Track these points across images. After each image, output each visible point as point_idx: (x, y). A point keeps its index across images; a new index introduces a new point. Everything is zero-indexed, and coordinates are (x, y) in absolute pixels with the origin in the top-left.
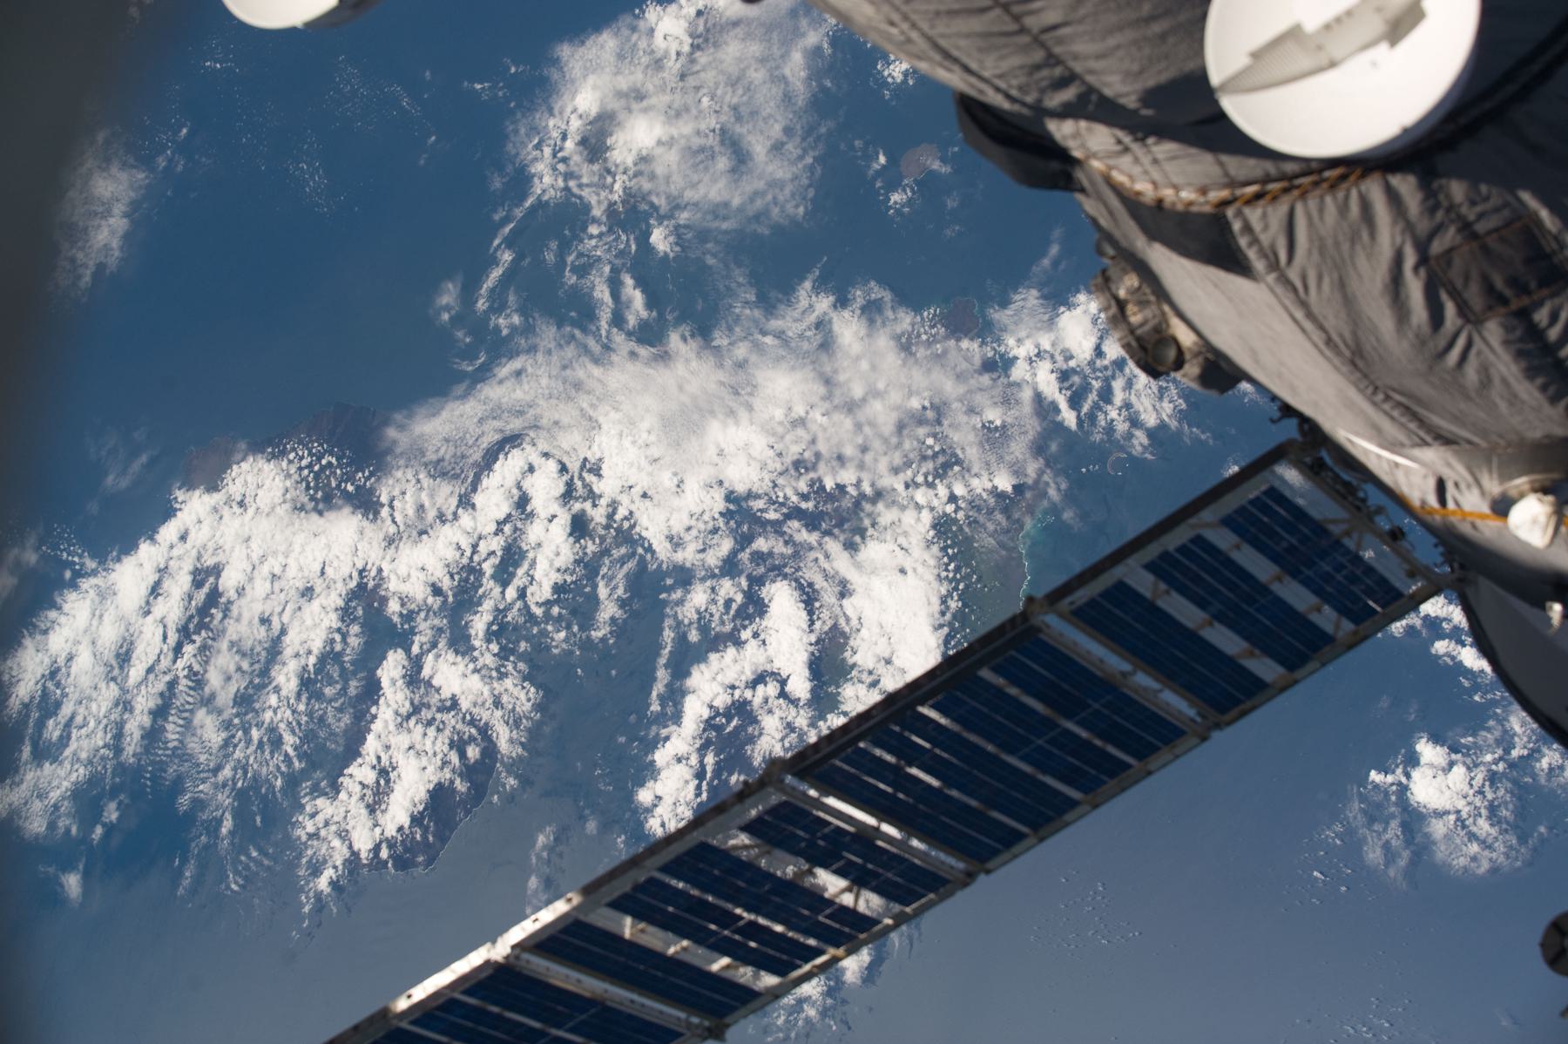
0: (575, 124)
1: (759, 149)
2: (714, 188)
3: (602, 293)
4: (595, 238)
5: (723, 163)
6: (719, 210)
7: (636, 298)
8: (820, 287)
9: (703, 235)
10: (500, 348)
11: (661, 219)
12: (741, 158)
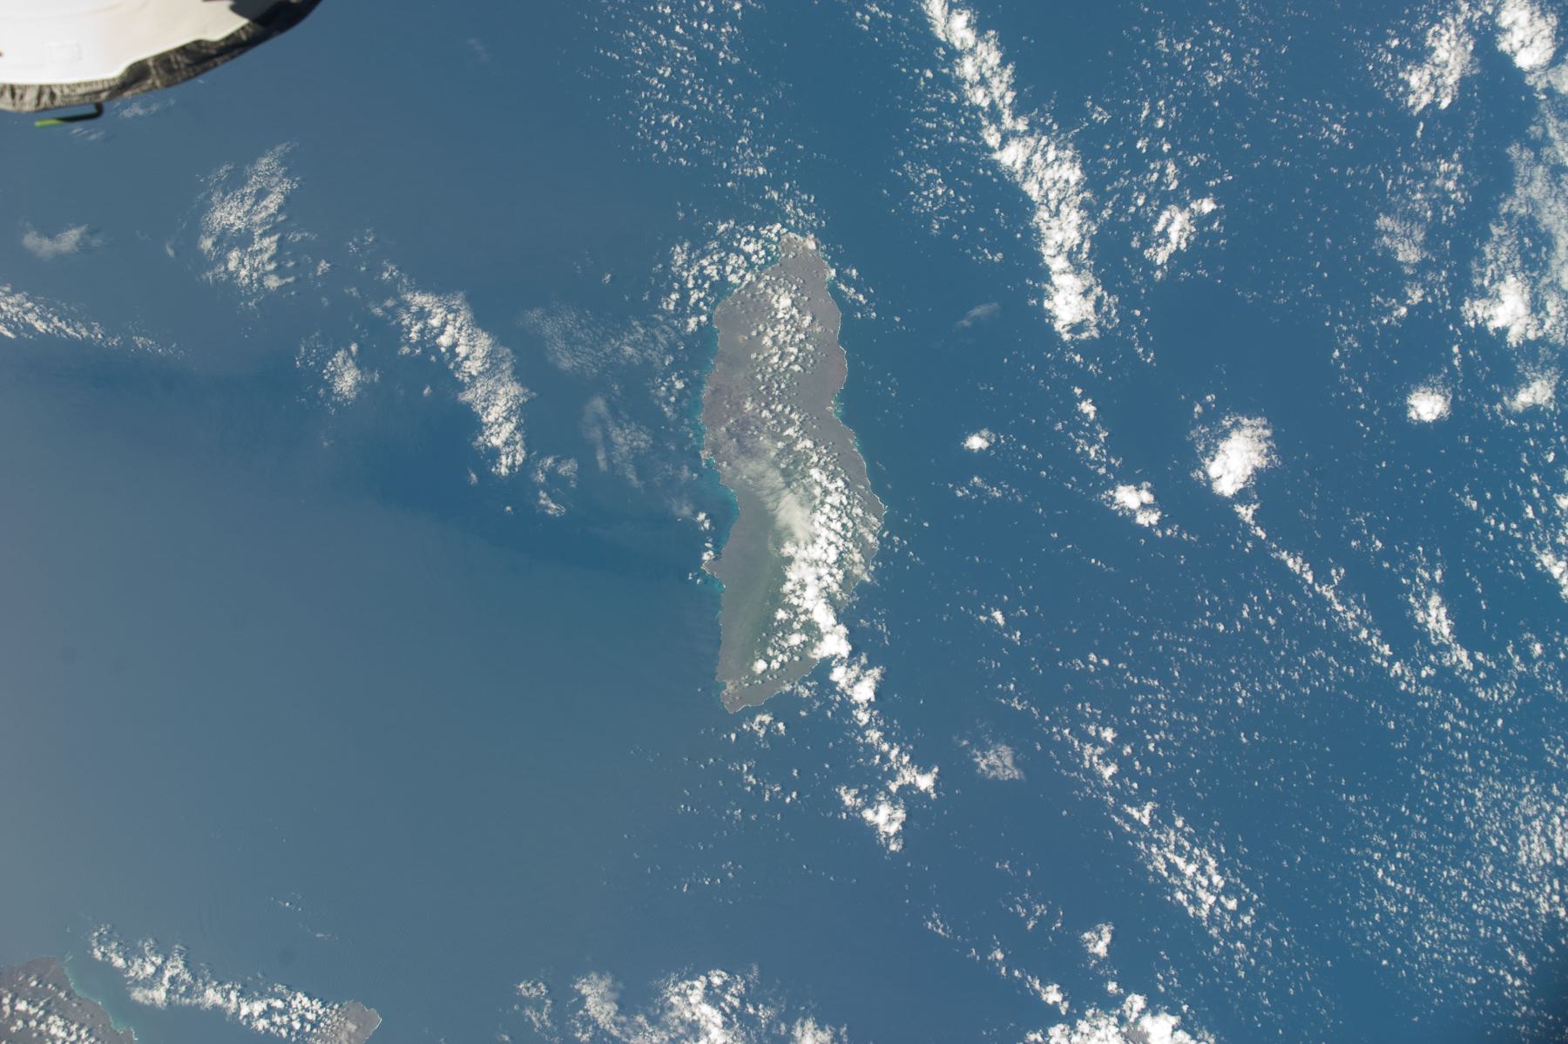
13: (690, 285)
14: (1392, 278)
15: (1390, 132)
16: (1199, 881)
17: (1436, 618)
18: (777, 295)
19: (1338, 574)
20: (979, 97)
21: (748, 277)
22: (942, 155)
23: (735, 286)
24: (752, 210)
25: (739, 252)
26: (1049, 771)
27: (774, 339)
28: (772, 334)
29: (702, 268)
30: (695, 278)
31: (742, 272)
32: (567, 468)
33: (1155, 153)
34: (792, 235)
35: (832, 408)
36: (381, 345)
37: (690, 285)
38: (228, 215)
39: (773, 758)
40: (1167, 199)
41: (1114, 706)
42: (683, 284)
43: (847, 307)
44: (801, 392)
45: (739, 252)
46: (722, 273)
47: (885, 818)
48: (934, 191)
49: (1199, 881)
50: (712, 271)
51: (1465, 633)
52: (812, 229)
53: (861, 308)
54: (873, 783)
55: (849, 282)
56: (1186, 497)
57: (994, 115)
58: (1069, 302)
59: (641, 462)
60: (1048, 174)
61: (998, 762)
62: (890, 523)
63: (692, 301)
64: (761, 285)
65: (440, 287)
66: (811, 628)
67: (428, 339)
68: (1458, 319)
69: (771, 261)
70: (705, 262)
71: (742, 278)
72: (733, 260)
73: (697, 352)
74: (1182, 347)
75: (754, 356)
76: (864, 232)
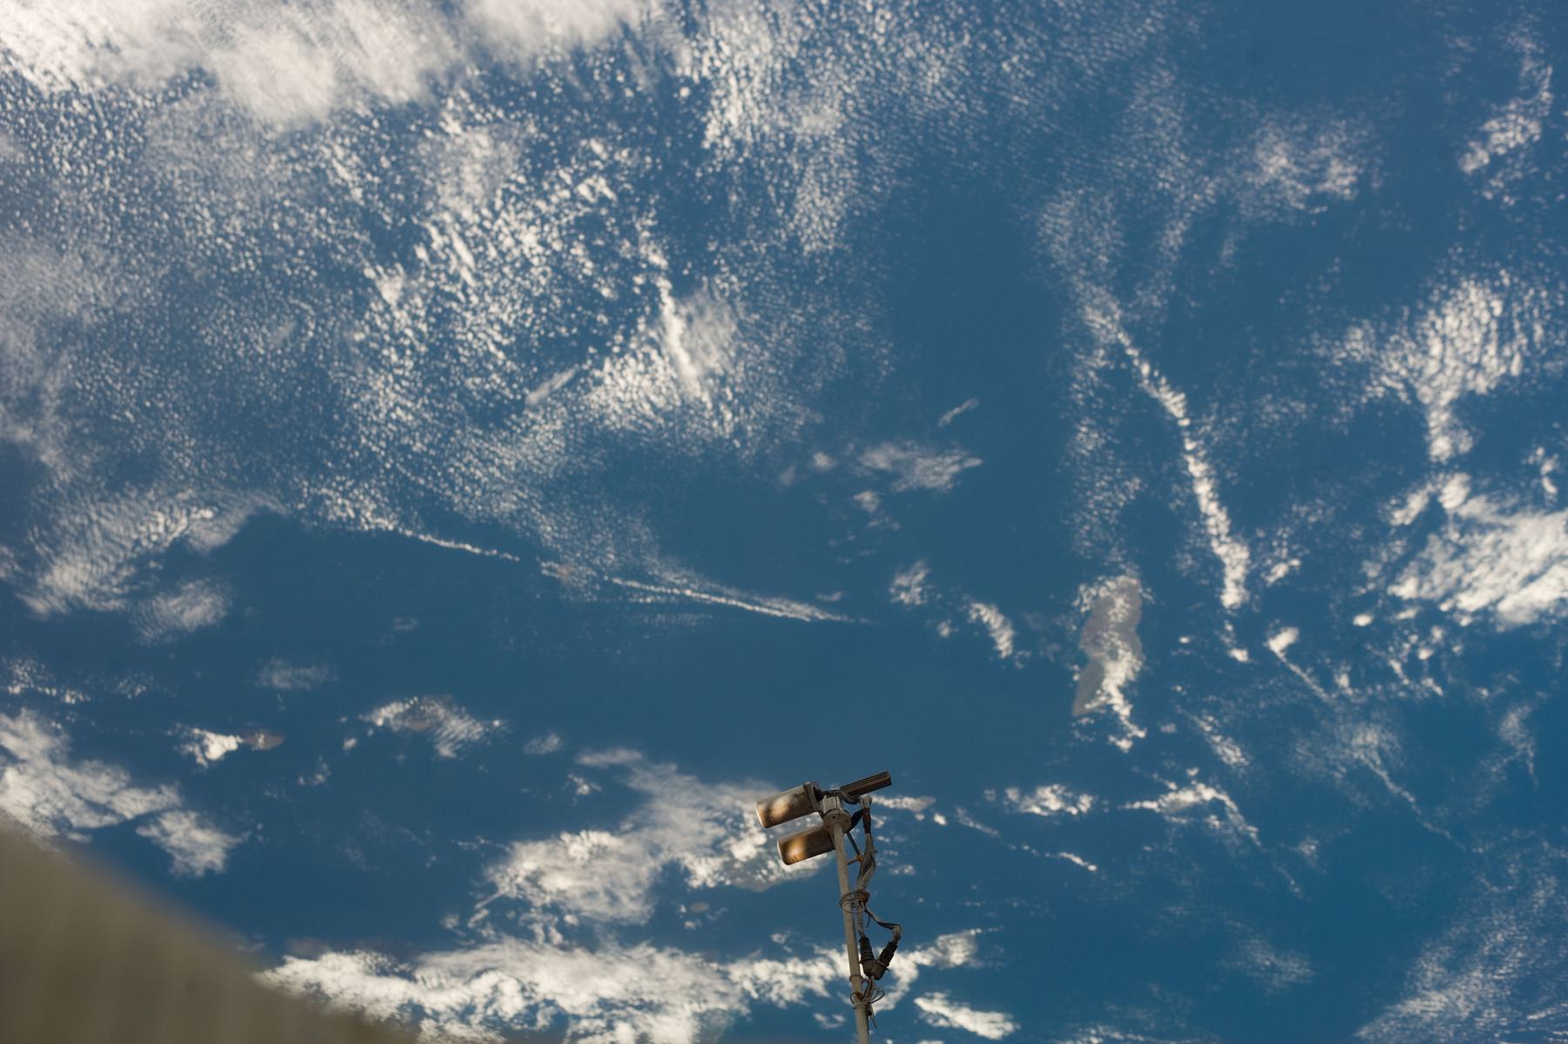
0: (523, 873)
1: (625, 900)
2: (601, 907)
3: (538, 929)
4: (534, 914)
5: (604, 899)
6: (600, 914)
7: (557, 937)
8: (652, 944)
9: (594, 921)
10: (481, 941)
11: (570, 912)
12: (614, 899)
14: (1364, 580)
15: (1381, 532)
16: (1232, 755)
17: (1344, 681)
18: (1117, 597)
19: (1309, 670)
20: (1214, 531)
22: (1193, 551)
24: (1113, 571)
26: (1186, 729)
32: (1028, 654)
33: (1280, 546)
35: (1132, 630)
36: (960, 619)
38: (902, 581)
39: (1087, 730)
40: (1278, 560)
41: (1215, 709)
44: (1121, 628)
47: (1124, 744)
48: (1187, 562)
49: (1232, 755)
51: (1352, 685)
54: (1122, 734)
56: (1261, 654)
57: (1218, 536)
58: (1231, 596)
59: (1055, 654)
60: (1234, 558)
61: (1170, 728)
62: (1146, 663)
65: (987, 602)
66: (1109, 696)
67: (979, 619)
68: (1384, 592)
73: (1082, 620)
74: (1269, 605)
76: (1155, 572)
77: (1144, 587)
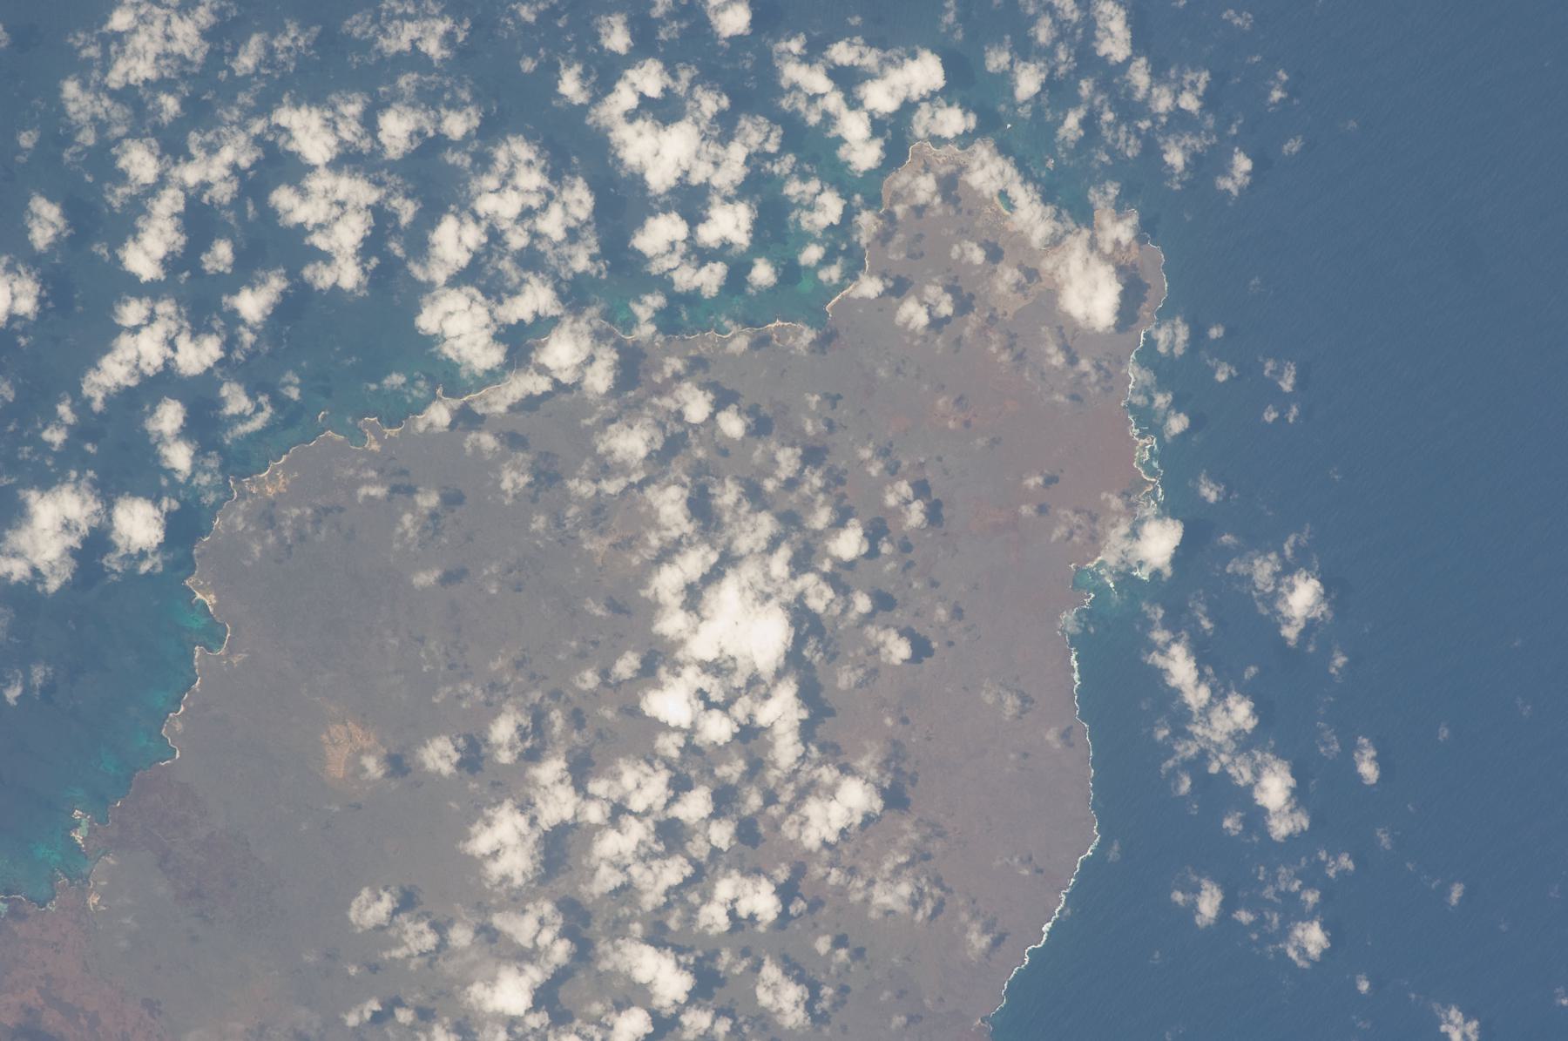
13: (144, 257)
21: (562, 353)
23: (448, 377)
25: (576, 148)
27: (560, 849)
28: (558, 805)
29: (279, 165)
30: (199, 220)
31: (536, 298)
34: (988, 172)
37: (144, 257)
42: (100, 221)
43: (1155, 812)
45: (576, 148)
46: (392, 253)
50: (332, 216)
52: (1140, 184)
53: (1244, 859)
55: (1240, 644)
63: (113, 372)
64: (631, 443)
69: (777, 287)
70: (310, 133)
71: (519, 343)
72: (515, 192)
75: (372, 909)
77: (1238, 480)
